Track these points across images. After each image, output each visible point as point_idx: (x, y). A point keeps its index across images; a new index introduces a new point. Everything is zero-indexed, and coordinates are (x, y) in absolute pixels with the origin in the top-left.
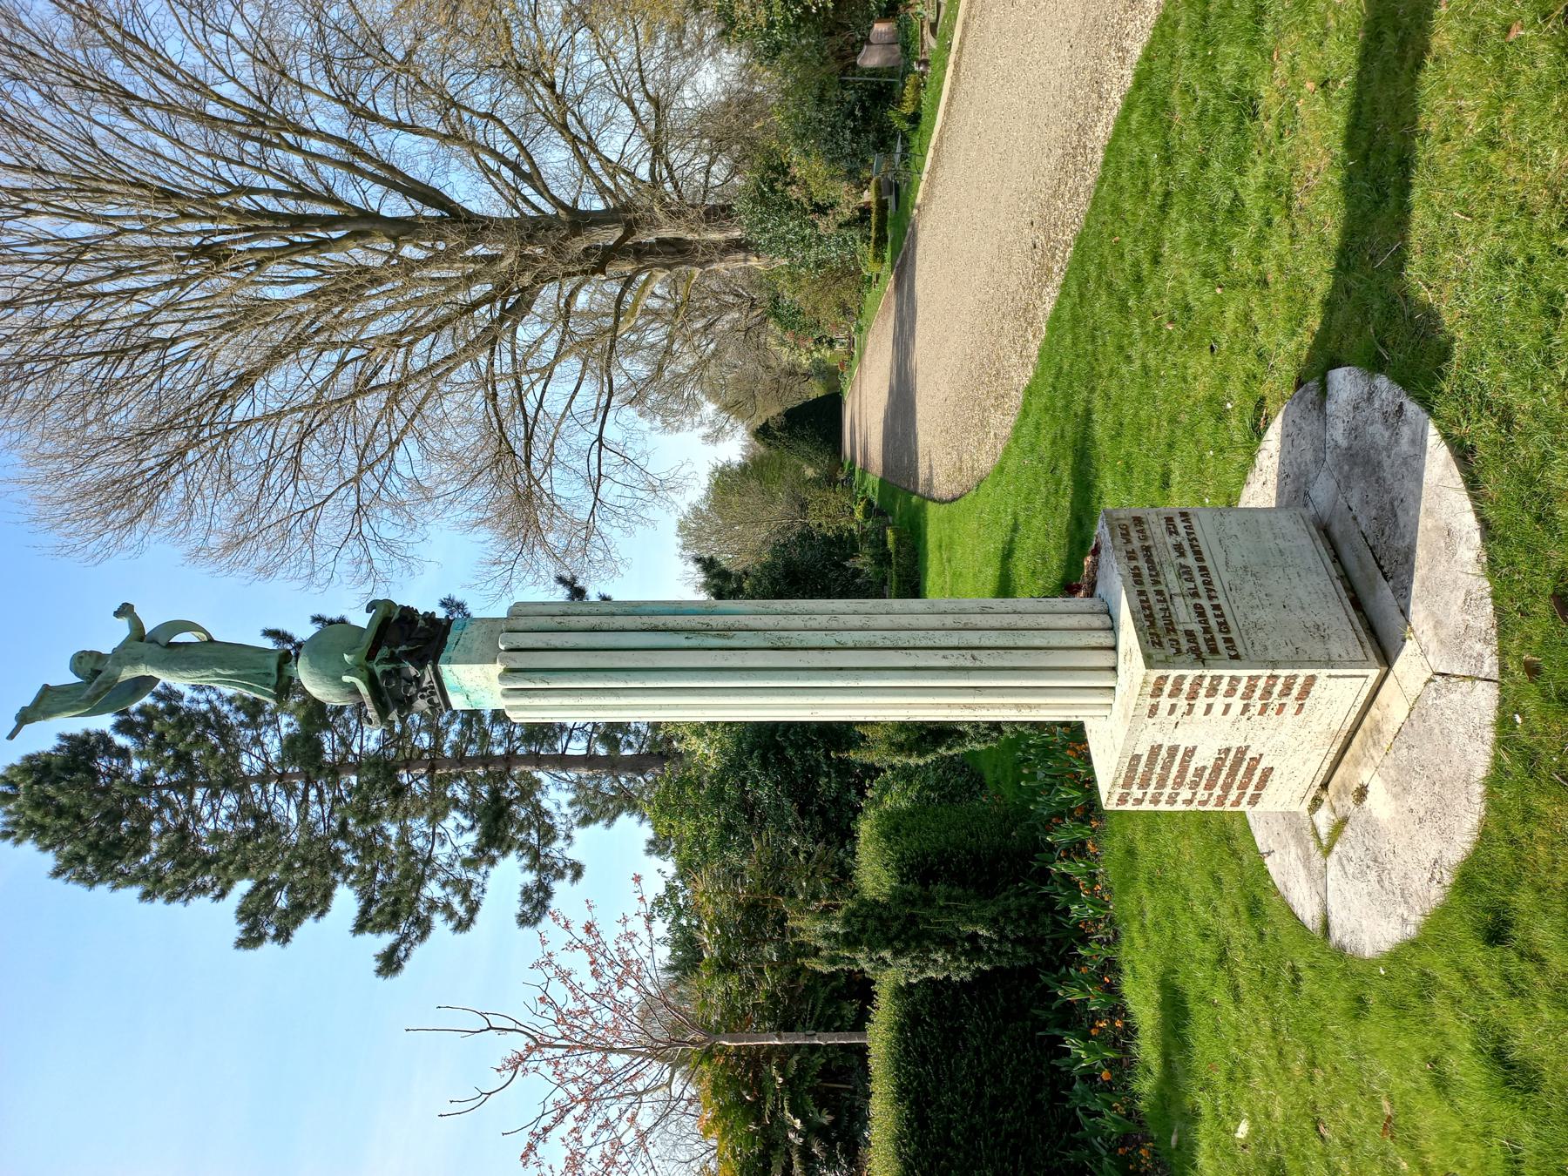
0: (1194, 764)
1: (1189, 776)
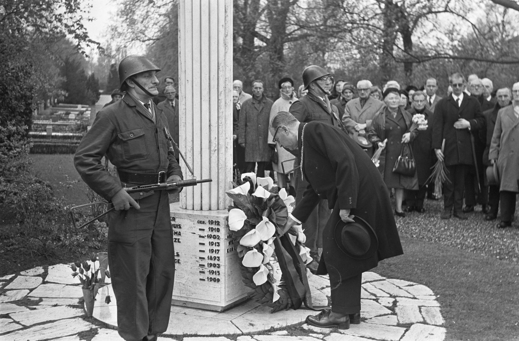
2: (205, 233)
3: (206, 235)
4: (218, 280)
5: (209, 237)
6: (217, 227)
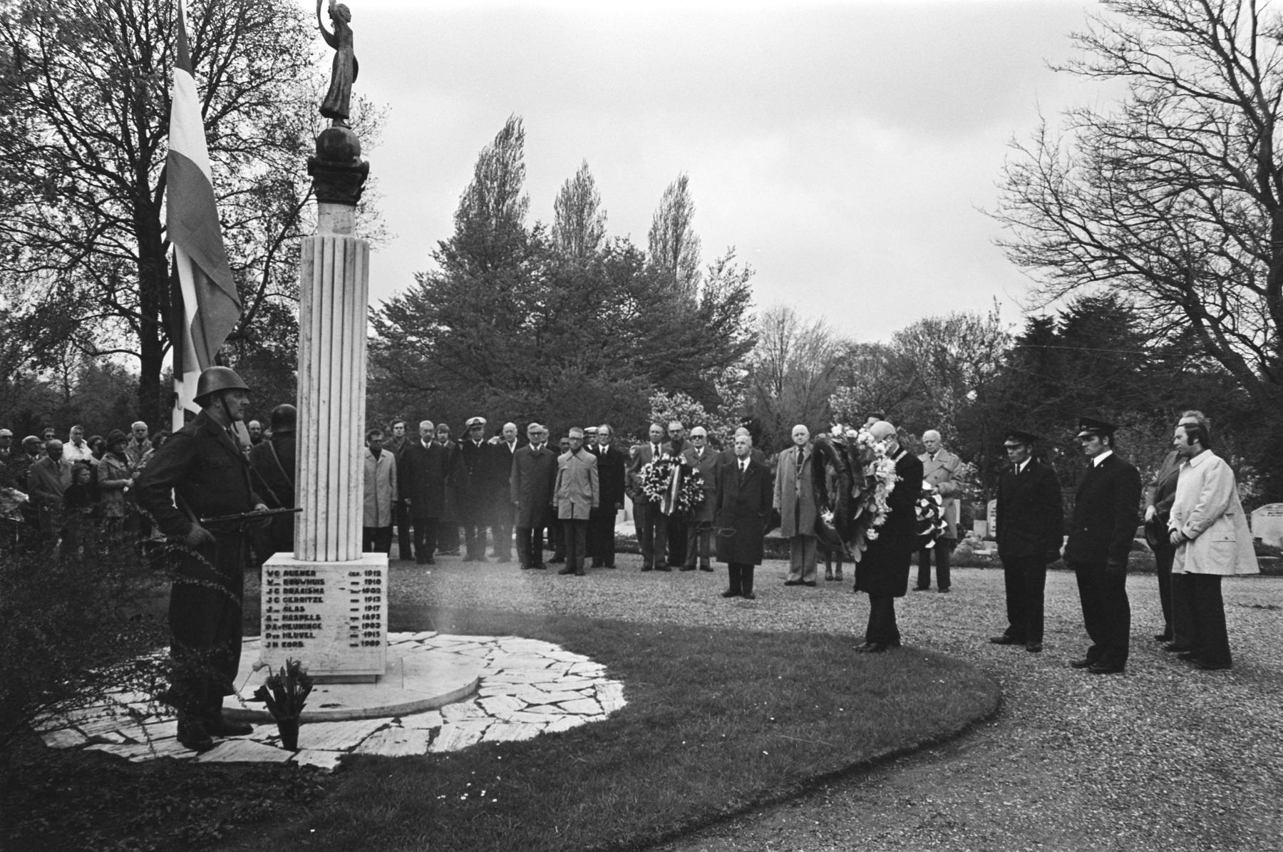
0: (304, 605)
1: (293, 606)
2: (360, 588)
5: (366, 591)
6: (376, 578)
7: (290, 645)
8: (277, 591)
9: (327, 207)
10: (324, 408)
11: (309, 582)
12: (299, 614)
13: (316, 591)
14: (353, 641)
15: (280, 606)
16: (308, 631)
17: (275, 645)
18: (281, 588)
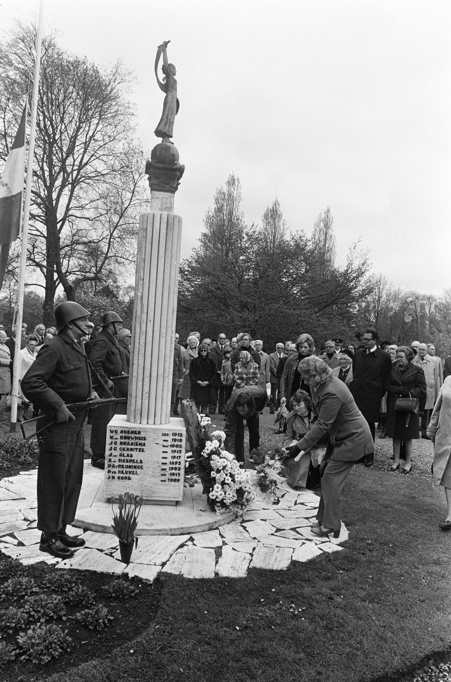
1: (126, 453)
2: (169, 443)
3: (170, 444)
4: (178, 480)
5: (172, 446)
6: (179, 438)
7: (122, 478)
8: (116, 443)
9: (157, 193)
10: (150, 325)
11: (136, 438)
12: (129, 458)
13: (141, 444)
14: (163, 478)
15: (117, 453)
16: (133, 470)
17: (113, 478)
18: (119, 441)
